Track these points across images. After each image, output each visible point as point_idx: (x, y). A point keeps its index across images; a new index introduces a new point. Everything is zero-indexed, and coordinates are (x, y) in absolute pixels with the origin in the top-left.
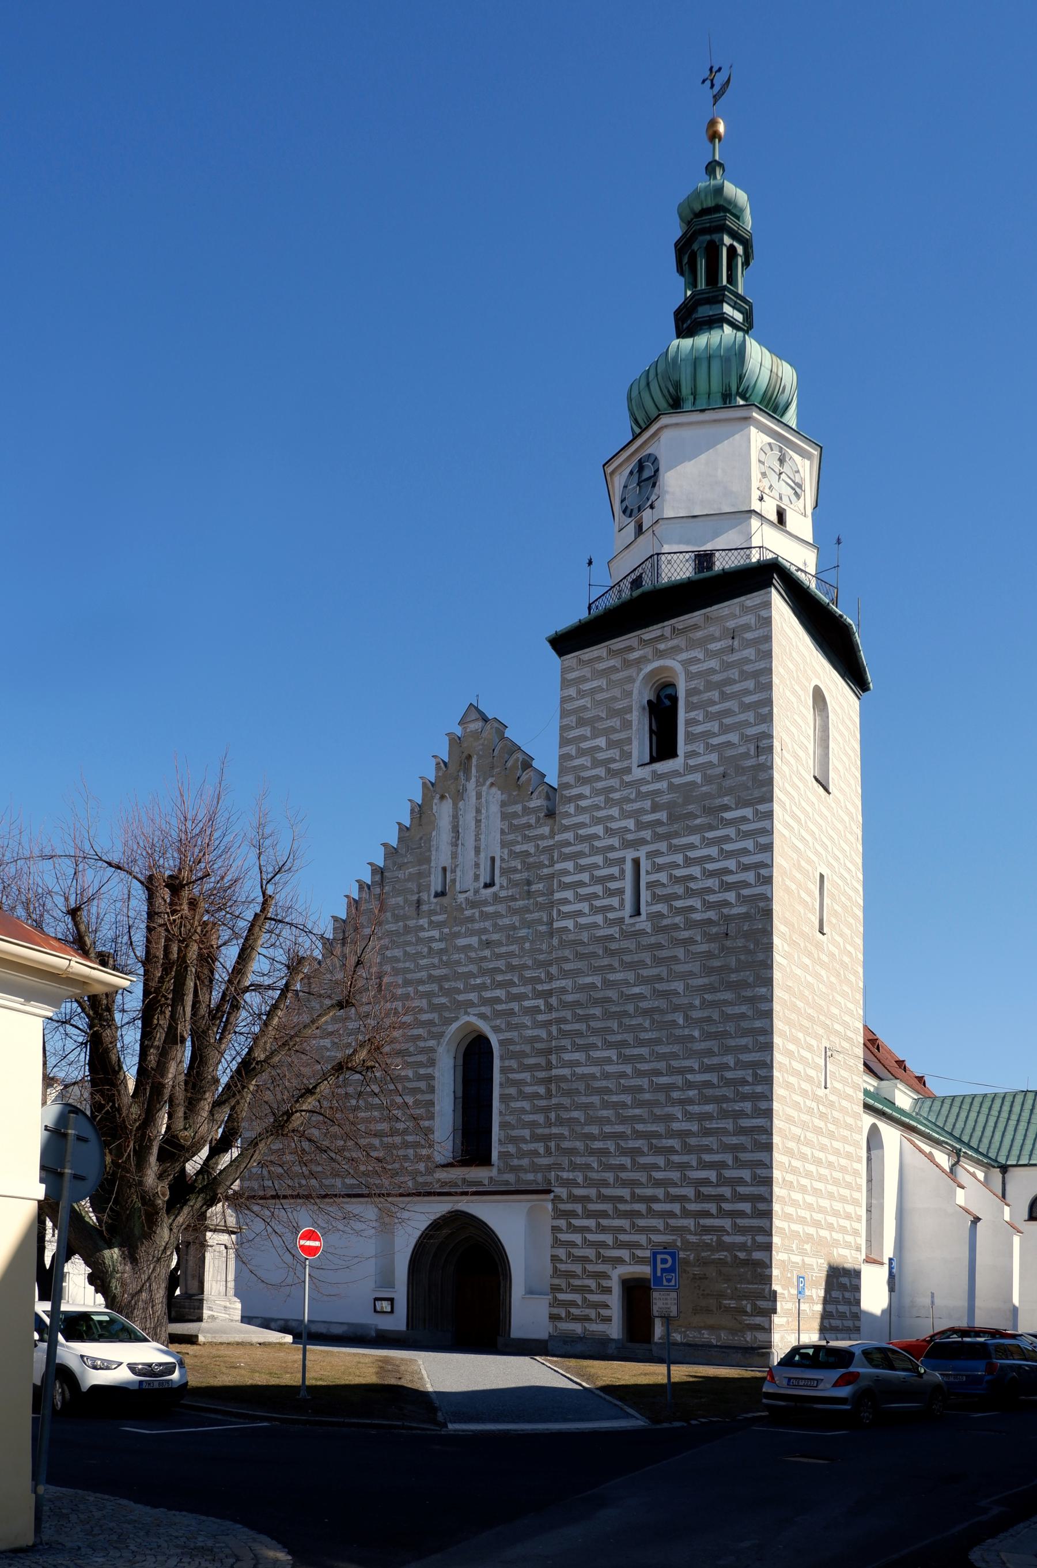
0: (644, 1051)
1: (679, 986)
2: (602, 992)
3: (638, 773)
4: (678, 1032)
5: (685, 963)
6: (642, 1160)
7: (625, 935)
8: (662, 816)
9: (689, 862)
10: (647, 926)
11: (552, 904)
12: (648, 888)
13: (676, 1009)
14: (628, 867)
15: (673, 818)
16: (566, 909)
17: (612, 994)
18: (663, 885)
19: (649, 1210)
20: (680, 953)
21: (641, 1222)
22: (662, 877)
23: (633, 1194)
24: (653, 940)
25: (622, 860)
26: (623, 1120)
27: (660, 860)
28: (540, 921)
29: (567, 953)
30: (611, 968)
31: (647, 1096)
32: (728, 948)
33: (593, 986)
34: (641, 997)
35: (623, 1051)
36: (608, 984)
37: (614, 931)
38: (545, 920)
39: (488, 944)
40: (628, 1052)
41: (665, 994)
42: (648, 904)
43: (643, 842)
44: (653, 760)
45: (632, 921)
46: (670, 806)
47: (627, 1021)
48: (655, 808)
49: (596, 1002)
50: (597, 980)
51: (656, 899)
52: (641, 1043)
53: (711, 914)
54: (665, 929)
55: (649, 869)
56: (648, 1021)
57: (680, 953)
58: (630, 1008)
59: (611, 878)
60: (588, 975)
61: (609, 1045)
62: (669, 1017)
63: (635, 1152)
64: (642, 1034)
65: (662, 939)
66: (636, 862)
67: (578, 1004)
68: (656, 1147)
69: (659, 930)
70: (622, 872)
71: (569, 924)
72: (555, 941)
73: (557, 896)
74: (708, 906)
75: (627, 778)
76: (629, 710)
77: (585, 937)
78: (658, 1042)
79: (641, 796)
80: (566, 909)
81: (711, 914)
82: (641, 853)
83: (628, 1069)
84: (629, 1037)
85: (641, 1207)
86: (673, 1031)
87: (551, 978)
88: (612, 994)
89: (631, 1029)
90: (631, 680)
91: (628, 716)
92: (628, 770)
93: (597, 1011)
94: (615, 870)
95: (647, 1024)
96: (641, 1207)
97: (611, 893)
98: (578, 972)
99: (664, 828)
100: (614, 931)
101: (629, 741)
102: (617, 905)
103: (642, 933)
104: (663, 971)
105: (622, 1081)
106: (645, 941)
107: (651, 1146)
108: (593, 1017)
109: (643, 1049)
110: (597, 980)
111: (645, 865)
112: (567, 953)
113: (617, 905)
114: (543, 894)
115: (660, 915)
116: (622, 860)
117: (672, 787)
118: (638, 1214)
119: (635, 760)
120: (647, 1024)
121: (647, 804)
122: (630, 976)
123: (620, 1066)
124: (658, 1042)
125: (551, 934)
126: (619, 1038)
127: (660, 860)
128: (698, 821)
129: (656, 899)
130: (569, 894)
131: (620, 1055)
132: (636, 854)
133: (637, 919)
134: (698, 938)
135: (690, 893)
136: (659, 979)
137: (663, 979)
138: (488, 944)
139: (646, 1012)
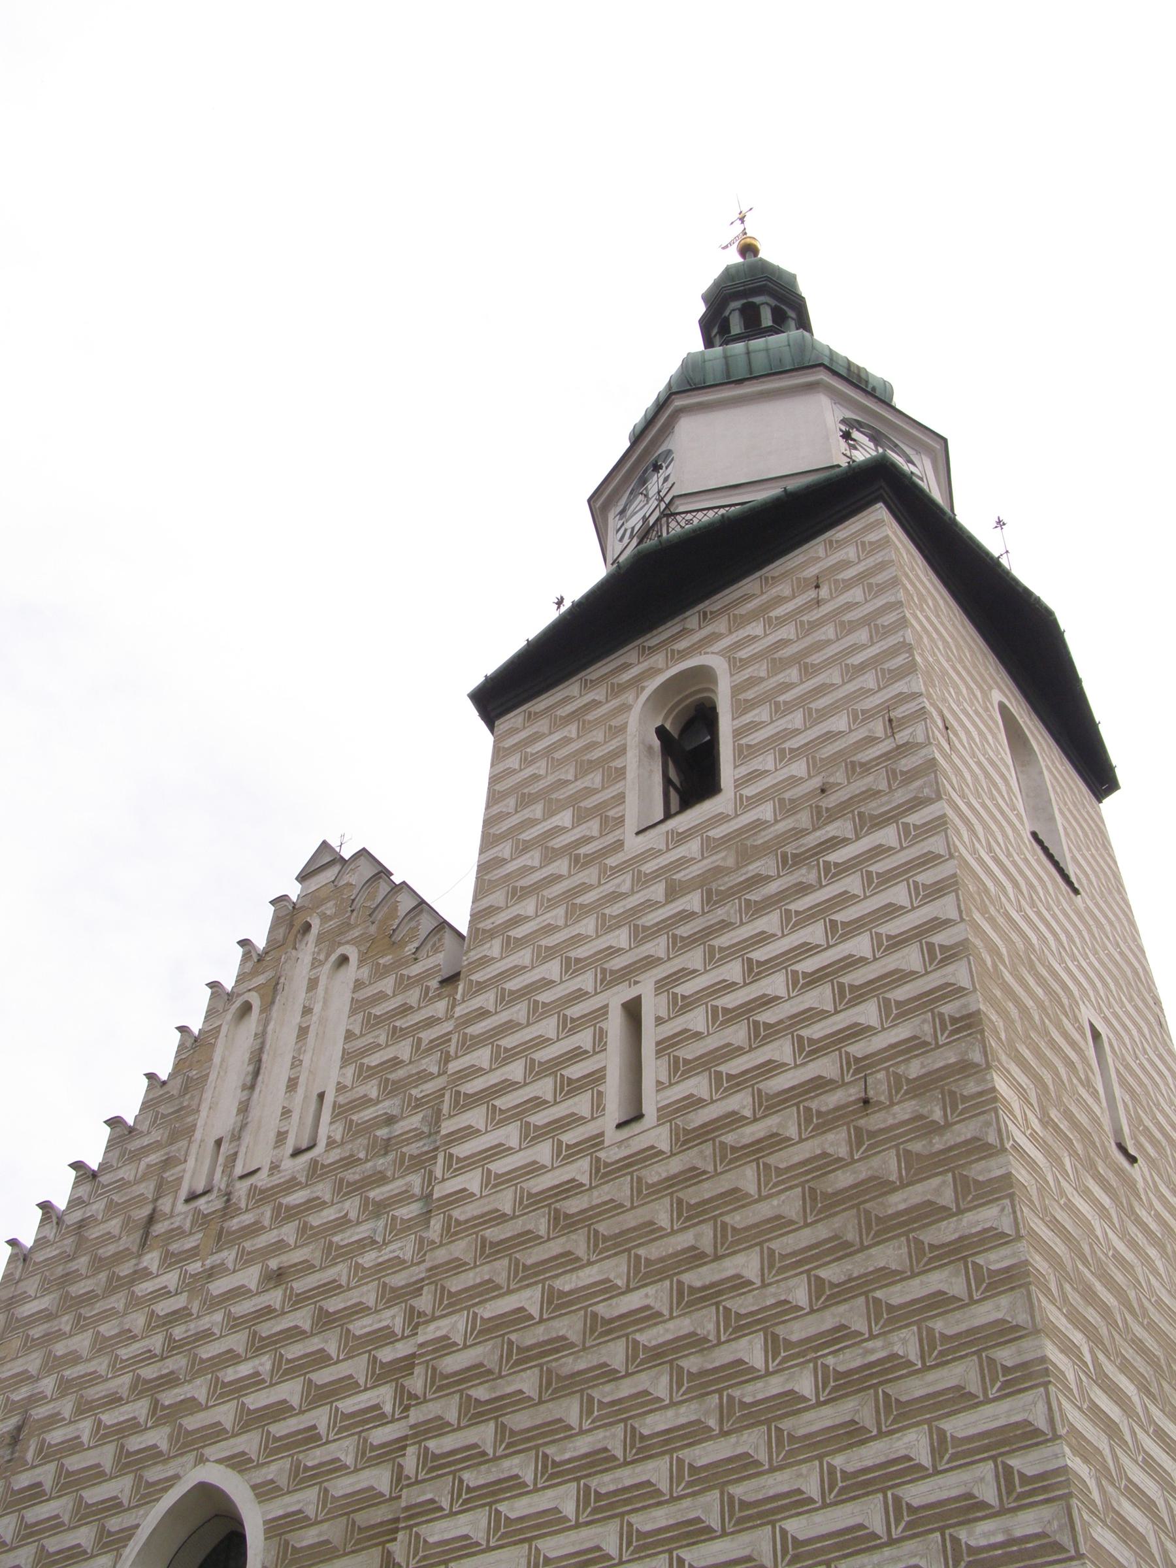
0: (656, 1471)
1: (747, 1264)
2: (541, 1329)
3: (635, 845)
4: (751, 1393)
5: (761, 1199)
7: (603, 1172)
8: (693, 901)
9: (755, 972)
10: (661, 1138)
12: (659, 1053)
13: (739, 1326)
14: (615, 1024)
15: (712, 899)
16: (462, 1150)
17: (569, 1327)
18: (697, 1035)
22: (697, 1020)
24: (675, 1166)
25: (603, 1011)
27: (687, 988)
28: (404, 1197)
29: (461, 1249)
30: (568, 1262)
33: (519, 1317)
34: (647, 1317)
35: (594, 1483)
37: (580, 1170)
40: (605, 1483)
41: (709, 1295)
42: (660, 1086)
44: (668, 816)
45: (626, 1132)
47: (606, 1393)
48: (673, 892)
49: (523, 1357)
50: (530, 1299)
51: (680, 1069)
52: (643, 1448)
53: (826, 1066)
56: (665, 1379)
57: (747, 1178)
59: (577, 1055)
60: (510, 1292)
62: (723, 1356)
64: (650, 1419)
65: (700, 1157)
66: (633, 1010)
67: (477, 1373)
69: (686, 1139)
70: (600, 1037)
71: (472, 1181)
73: (447, 1127)
74: (811, 1050)
76: (622, 751)
77: (505, 1201)
78: (695, 1433)
79: (641, 881)
80: (462, 1150)
81: (826, 1066)
82: (645, 988)
84: (613, 1439)
86: (736, 1393)
87: (415, 1320)
88: (569, 1327)
89: (622, 1412)
90: (626, 708)
91: (618, 763)
92: (619, 845)
93: (527, 1382)
94: (584, 1039)
95: (661, 1386)
97: (570, 1088)
98: (488, 1290)
100: (580, 1170)
101: (621, 798)
102: (585, 1111)
104: (703, 1236)
106: (654, 1174)
109: (651, 1465)
110: (530, 1299)
112: (461, 1249)
113: (585, 1111)
116: (603, 1011)
117: (710, 846)
119: (631, 825)
120: (661, 1386)
121: (657, 891)
122: (616, 1269)
123: (585, 1532)
124: (695, 1433)
126: (583, 1445)
127: (687, 988)
128: (773, 888)
129: (680, 1069)
130: (476, 1117)
131: (584, 1497)
133: (636, 1128)
134: (792, 1131)
135: (762, 1034)
136: (694, 1257)
137: (703, 1255)
139: (658, 1355)
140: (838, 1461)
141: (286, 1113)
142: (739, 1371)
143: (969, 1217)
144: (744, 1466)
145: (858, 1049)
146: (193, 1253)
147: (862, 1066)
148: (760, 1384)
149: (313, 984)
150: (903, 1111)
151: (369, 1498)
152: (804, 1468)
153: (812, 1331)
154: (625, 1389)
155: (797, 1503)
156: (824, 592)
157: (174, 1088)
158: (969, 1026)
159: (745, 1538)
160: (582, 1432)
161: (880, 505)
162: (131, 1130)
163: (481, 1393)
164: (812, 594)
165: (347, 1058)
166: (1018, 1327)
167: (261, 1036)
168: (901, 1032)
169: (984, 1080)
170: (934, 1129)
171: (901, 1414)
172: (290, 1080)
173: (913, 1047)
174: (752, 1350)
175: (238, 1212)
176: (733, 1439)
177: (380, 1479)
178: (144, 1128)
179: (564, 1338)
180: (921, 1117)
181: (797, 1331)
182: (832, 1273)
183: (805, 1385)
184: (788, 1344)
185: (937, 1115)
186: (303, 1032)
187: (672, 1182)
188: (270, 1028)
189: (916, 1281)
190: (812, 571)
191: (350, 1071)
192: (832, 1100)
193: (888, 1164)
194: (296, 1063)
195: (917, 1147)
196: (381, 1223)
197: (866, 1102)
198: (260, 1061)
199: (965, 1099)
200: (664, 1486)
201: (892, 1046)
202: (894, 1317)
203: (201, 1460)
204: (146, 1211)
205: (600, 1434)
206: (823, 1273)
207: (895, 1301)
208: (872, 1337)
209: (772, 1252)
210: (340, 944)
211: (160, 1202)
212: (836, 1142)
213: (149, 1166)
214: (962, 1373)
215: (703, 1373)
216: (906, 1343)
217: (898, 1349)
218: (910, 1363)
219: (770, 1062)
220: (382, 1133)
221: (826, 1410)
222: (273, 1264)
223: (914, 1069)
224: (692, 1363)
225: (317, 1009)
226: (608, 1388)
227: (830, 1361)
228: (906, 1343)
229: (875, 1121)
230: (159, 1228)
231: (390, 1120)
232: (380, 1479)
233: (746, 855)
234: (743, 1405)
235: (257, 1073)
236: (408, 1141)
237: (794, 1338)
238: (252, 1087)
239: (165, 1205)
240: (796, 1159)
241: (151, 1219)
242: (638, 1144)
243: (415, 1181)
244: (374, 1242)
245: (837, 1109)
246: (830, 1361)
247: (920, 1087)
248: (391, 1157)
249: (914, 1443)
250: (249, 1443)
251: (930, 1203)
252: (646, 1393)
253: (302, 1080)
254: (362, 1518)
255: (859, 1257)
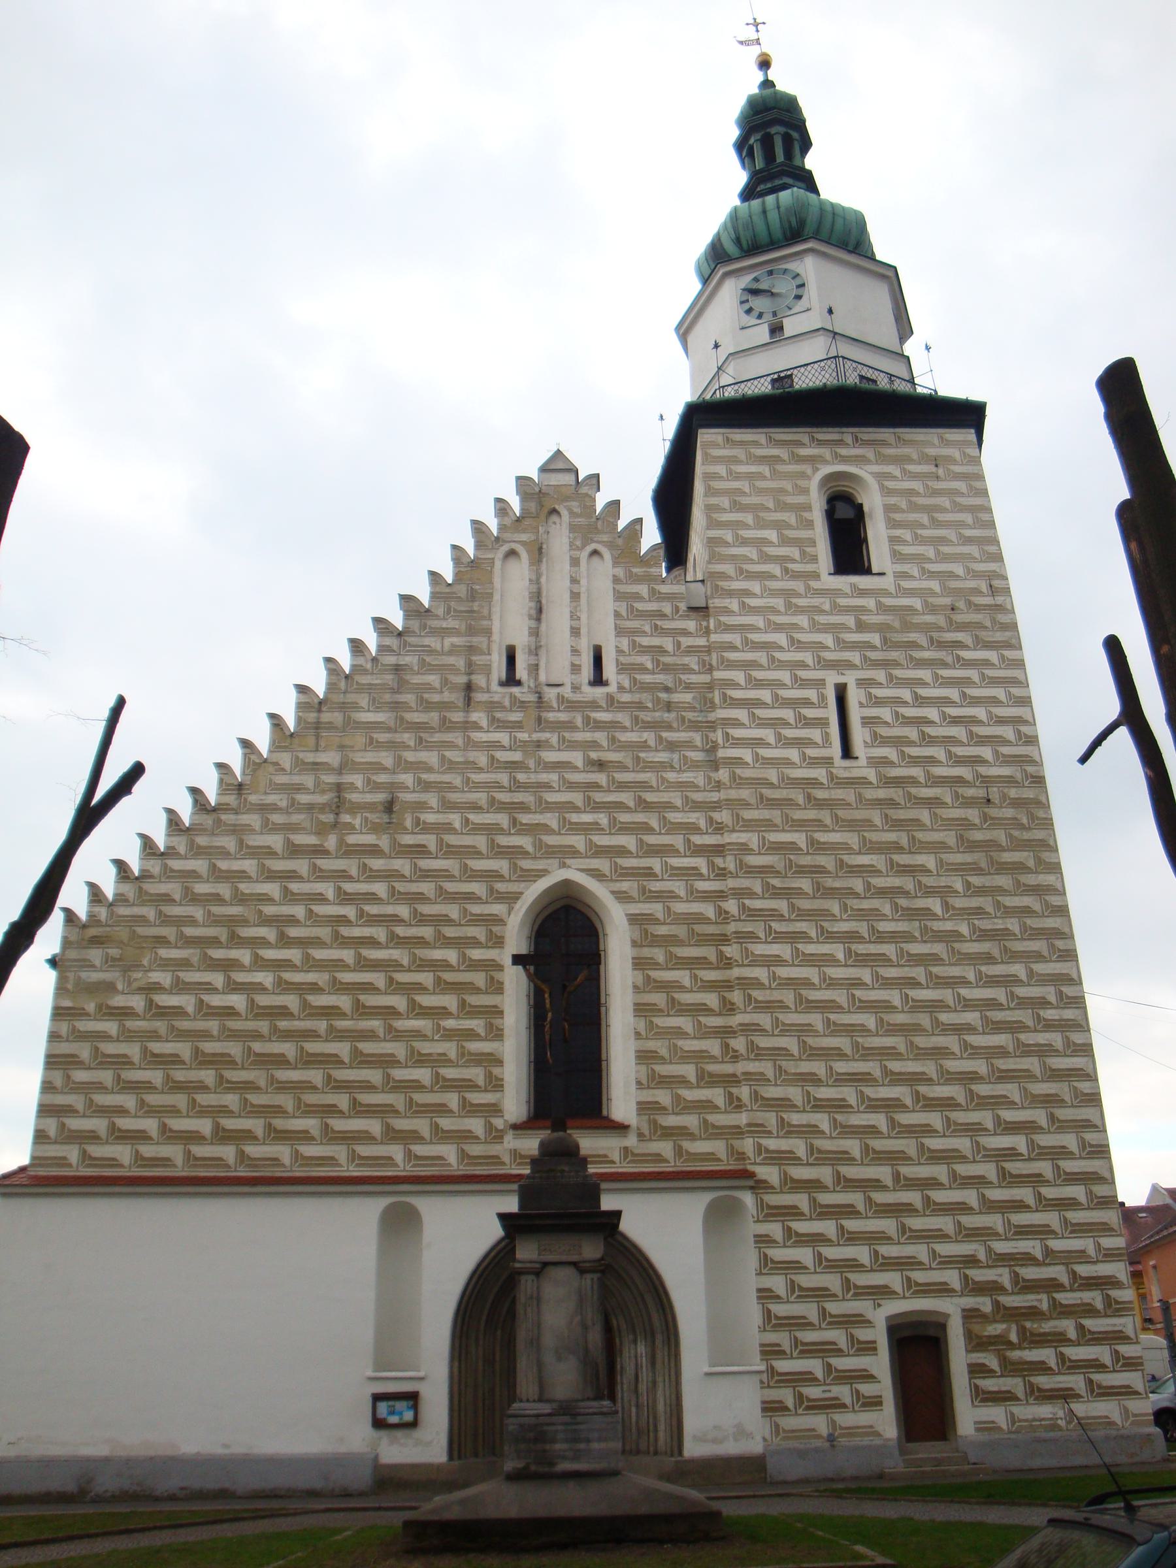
0: (889, 950)
1: (928, 861)
4: (937, 926)
6: (905, 1119)
7: (837, 782)
10: (871, 774)
11: (712, 726)
13: (930, 892)
19: (927, 1201)
20: (925, 816)
21: (916, 1223)
23: (897, 1176)
25: (821, 683)
26: (867, 1054)
31: (900, 1018)
32: (993, 819)
33: (792, 847)
35: (854, 947)
36: (817, 847)
38: (699, 744)
39: (601, 765)
43: (850, 665)
46: (882, 628)
51: (878, 740)
54: (898, 782)
55: (864, 701)
58: (858, 885)
60: (783, 831)
61: (830, 937)
63: (891, 1106)
64: (881, 923)
68: (925, 1098)
72: (723, 775)
75: (814, 584)
78: (907, 937)
83: (866, 975)
84: (863, 928)
85: (913, 1197)
86: (929, 924)
93: (805, 884)
94: (811, 694)
96: (913, 1197)
99: (877, 653)
103: (863, 782)
105: (858, 993)
107: (917, 1096)
108: (799, 892)
111: (854, 696)
112: (745, 794)
114: (692, 709)
115: (885, 762)
118: (908, 1209)
120: (887, 909)
122: (853, 840)
125: (715, 765)
126: (844, 927)
129: (878, 740)
131: (849, 953)
132: (841, 679)
136: (898, 848)
137: (902, 848)
138: (601, 765)
139: (882, 892)
140: (983, 968)
141: (575, 651)
142: (927, 913)
143: (1041, 877)
144: (935, 959)
145: (982, 770)
146: (518, 725)
147: (987, 781)
148: (940, 923)
149: (575, 562)
150: (1009, 813)
151: (701, 919)
152: (967, 968)
153: (966, 905)
154: (866, 904)
155: (963, 982)
156: (941, 472)
157: (462, 590)
158: (1040, 782)
159: (939, 991)
160: (841, 920)
161: (973, 431)
162: (428, 611)
163: (776, 882)
164: (933, 469)
165: (620, 632)
166: (1064, 933)
167: (536, 581)
168: (1005, 771)
169: (1046, 813)
170: (1022, 827)
171: (1014, 956)
172: (572, 628)
173: (1010, 781)
174: (935, 905)
175: (550, 709)
176: (929, 945)
177: (709, 911)
178: (440, 611)
179: (823, 867)
180: (1016, 819)
181: (959, 903)
182: (976, 880)
183: (964, 929)
184: (954, 908)
185: (1025, 821)
186: (575, 596)
187: (879, 803)
188: (543, 580)
189: (1016, 898)
190: (932, 452)
191: (625, 643)
192: (970, 792)
193: (1000, 836)
194: (574, 616)
195: (1016, 833)
196: (676, 756)
197: (989, 800)
198: (540, 602)
199: (1038, 818)
200: (894, 958)
201: (999, 776)
202: (1009, 912)
203: (563, 865)
204: (462, 680)
205: (854, 924)
206: (970, 879)
207: (1008, 904)
208: (996, 917)
209: (941, 860)
210: (592, 541)
211: (473, 677)
212: (973, 815)
213: (453, 645)
214: (1039, 945)
215: (909, 909)
216: (1013, 925)
217: (1009, 926)
218: (1015, 935)
219: (932, 757)
220: (663, 696)
221: (976, 944)
222: (594, 755)
223: (1013, 793)
224: (903, 902)
225: (583, 582)
226: (855, 901)
227: (976, 922)
228: (1013, 925)
229: (993, 812)
230: (479, 697)
231: (667, 689)
232: (709, 911)
233: (907, 626)
234: (933, 931)
235: (540, 611)
236: (685, 709)
237: (957, 906)
238: (539, 620)
239: (479, 680)
240: (951, 816)
241: (469, 688)
242: (856, 773)
243: (697, 738)
244: (672, 767)
245: (972, 798)
246: (976, 922)
247: (1017, 803)
248: (673, 715)
249: (1019, 970)
250: (603, 864)
251: (1021, 863)
252: (877, 910)
253: (584, 631)
254: (698, 928)
255: (989, 877)
